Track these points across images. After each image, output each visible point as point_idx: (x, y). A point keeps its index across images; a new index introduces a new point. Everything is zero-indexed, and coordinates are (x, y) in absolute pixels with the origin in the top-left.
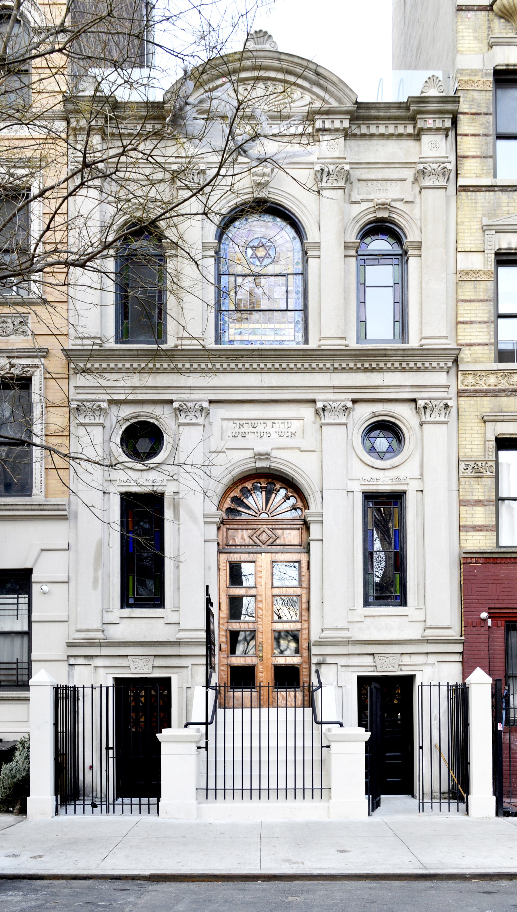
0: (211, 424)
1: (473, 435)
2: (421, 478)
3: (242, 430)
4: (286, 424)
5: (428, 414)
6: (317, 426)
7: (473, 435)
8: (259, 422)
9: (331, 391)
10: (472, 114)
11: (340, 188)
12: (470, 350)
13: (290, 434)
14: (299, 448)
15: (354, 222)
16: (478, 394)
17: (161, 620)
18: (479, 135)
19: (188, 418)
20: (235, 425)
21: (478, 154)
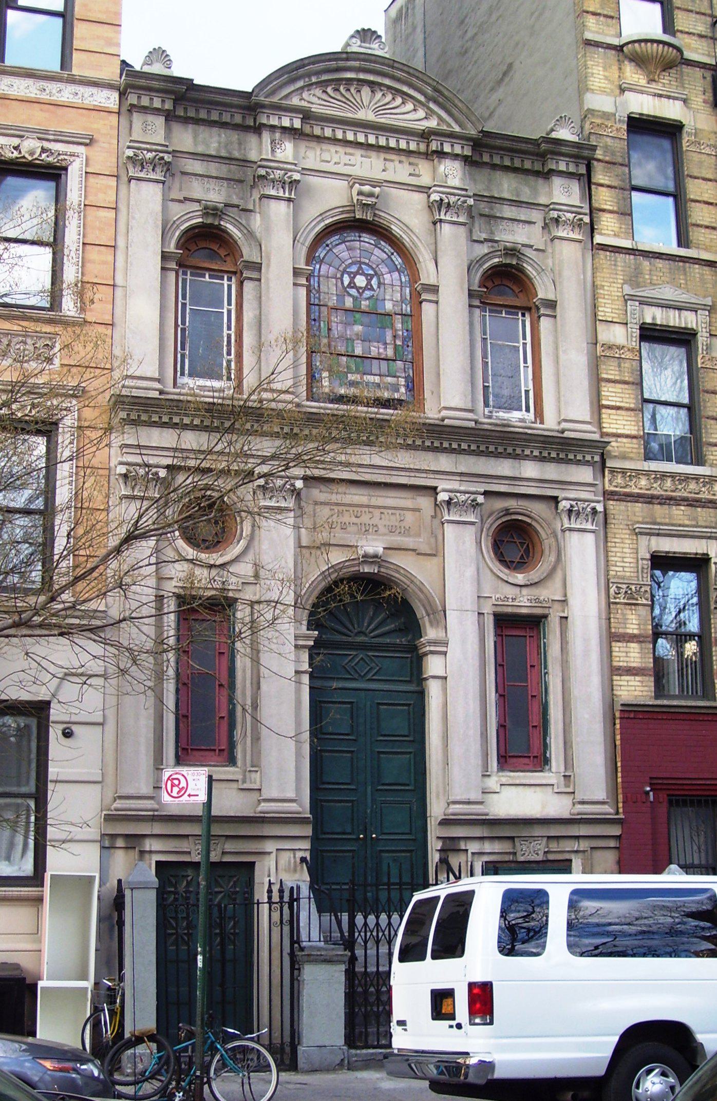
1: (625, 550)
2: (564, 602)
6: (436, 522)
7: (625, 550)
9: (458, 478)
10: (606, 162)
12: (617, 441)
13: (403, 530)
14: (414, 550)
16: (629, 499)
17: (234, 785)
18: (615, 187)
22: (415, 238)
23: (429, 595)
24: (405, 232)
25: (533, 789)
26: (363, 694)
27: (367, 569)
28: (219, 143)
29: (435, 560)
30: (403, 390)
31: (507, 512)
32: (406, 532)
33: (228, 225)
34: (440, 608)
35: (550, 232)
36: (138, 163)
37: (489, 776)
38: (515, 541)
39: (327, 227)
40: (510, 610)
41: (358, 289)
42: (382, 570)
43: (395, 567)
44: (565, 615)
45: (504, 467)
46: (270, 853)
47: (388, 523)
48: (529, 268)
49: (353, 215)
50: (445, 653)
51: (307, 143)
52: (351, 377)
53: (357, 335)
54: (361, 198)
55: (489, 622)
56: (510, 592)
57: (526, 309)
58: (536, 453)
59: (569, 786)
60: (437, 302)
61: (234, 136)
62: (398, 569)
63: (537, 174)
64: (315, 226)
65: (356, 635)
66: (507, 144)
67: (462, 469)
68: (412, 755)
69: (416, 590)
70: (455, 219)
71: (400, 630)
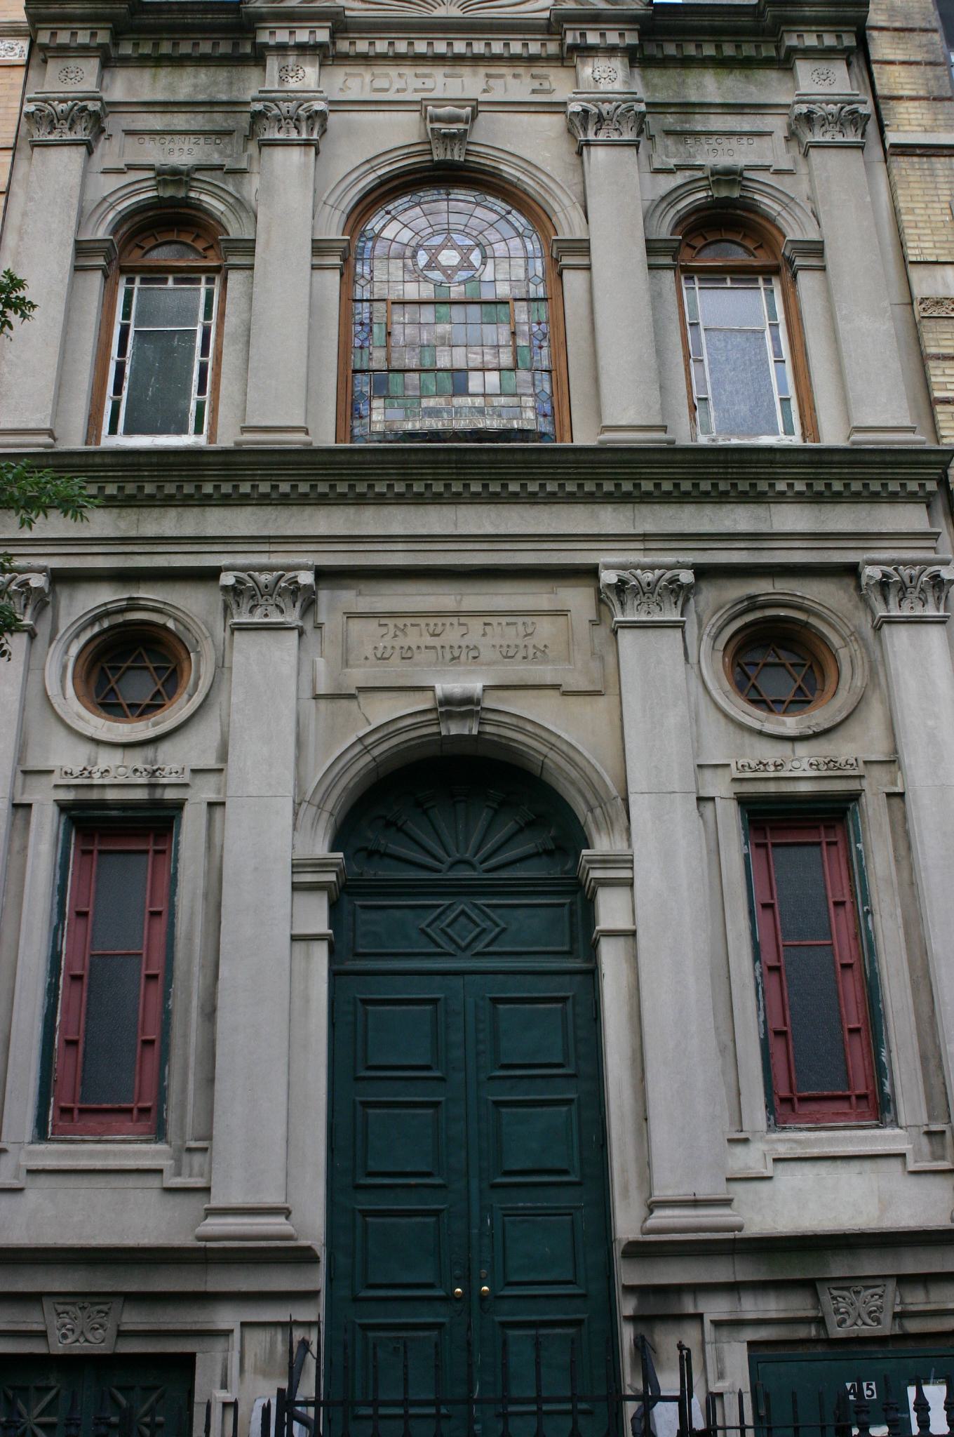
0: (318, 627)
2: (892, 762)
3: (402, 641)
4: (520, 628)
5: (893, 600)
6: (603, 631)
8: (448, 621)
11: (627, 144)
13: (531, 651)
14: (556, 687)
15: (664, 205)
17: (154, 1181)
19: (259, 611)
20: (384, 630)
21: (922, 93)
22: (543, 177)
23: (588, 770)
24: (525, 171)
25: (855, 1166)
26: (457, 982)
27: (455, 729)
28: (195, 86)
29: (601, 702)
30: (530, 414)
31: (753, 603)
32: (541, 654)
33: (203, 197)
34: (614, 792)
35: (800, 143)
36: (45, 122)
37: (746, 1141)
38: (777, 655)
39: (383, 182)
40: (772, 788)
41: (444, 269)
42: (488, 729)
43: (514, 721)
44: (898, 789)
45: (739, 518)
46: (227, 1333)
47: (497, 642)
48: (766, 201)
49: (427, 158)
50: (630, 883)
51: (348, 70)
52: (426, 403)
53: (443, 338)
54: (437, 125)
55: (730, 819)
56: (770, 753)
57: (769, 272)
58: (800, 486)
59: (943, 1158)
60: (588, 268)
61: (222, 74)
62: (521, 723)
63: (768, 63)
64: (358, 180)
65: (452, 866)
66: (706, 22)
67: (649, 528)
68: (574, 1108)
69: (562, 763)
70: (615, 137)
71: (549, 853)
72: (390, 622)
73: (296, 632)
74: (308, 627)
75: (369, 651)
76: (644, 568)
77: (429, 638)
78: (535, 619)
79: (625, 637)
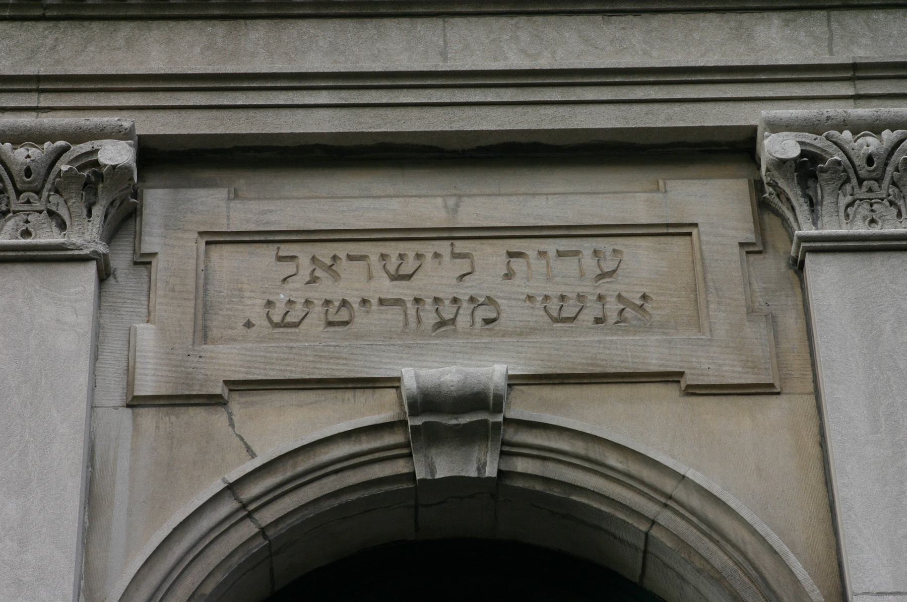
3: (327, 289)
4: (589, 261)
6: (772, 266)
8: (428, 249)
13: (613, 307)
20: (288, 268)
23: (752, 547)
27: (445, 465)
32: (636, 312)
42: (521, 465)
43: (579, 447)
47: (539, 288)
62: (595, 452)
67: (863, 53)
69: (692, 535)
72: (304, 253)
73: (91, 270)
74: (121, 261)
75: (256, 313)
76: (857, 128)
77: (387, 282)
78: (619, 243)
79: (823, 272)
